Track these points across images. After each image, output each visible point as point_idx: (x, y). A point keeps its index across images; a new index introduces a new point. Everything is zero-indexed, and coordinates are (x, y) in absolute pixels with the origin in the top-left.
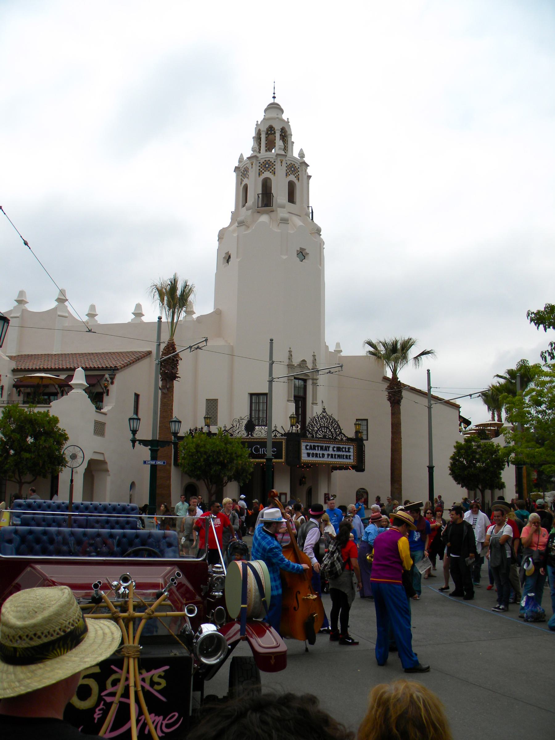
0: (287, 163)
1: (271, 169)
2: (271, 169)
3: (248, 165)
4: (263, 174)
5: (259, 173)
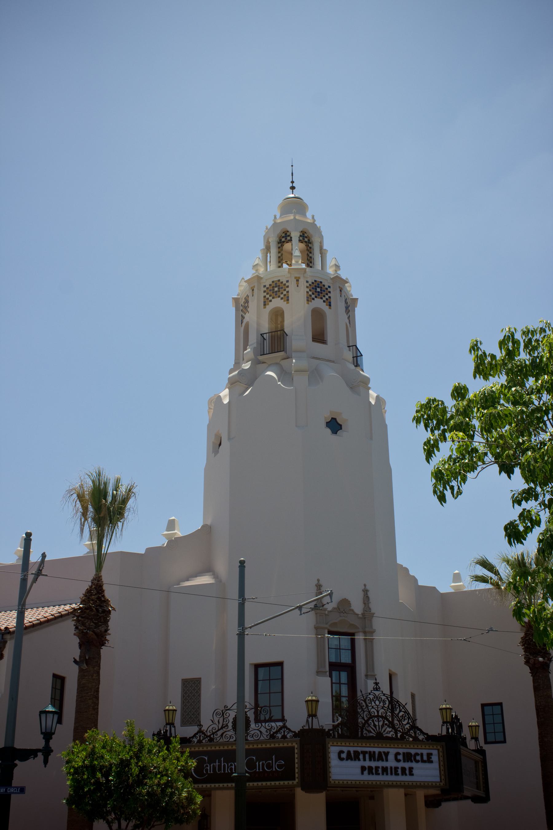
1: (282, 293)
2: (282, 293)
4: (270, 303)
5: (265, 302)
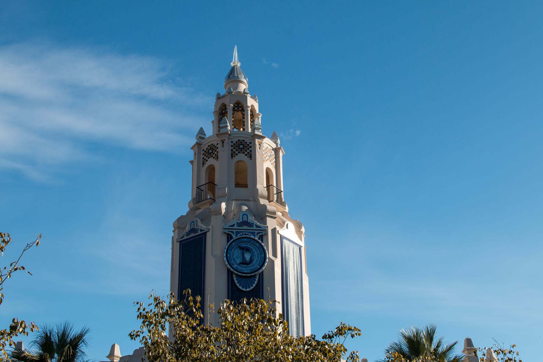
0: (217, 144)
1: (246, 151)
2: (246, 151)
3: (215, 143)
4: (236, 156)
5: (232, 154)
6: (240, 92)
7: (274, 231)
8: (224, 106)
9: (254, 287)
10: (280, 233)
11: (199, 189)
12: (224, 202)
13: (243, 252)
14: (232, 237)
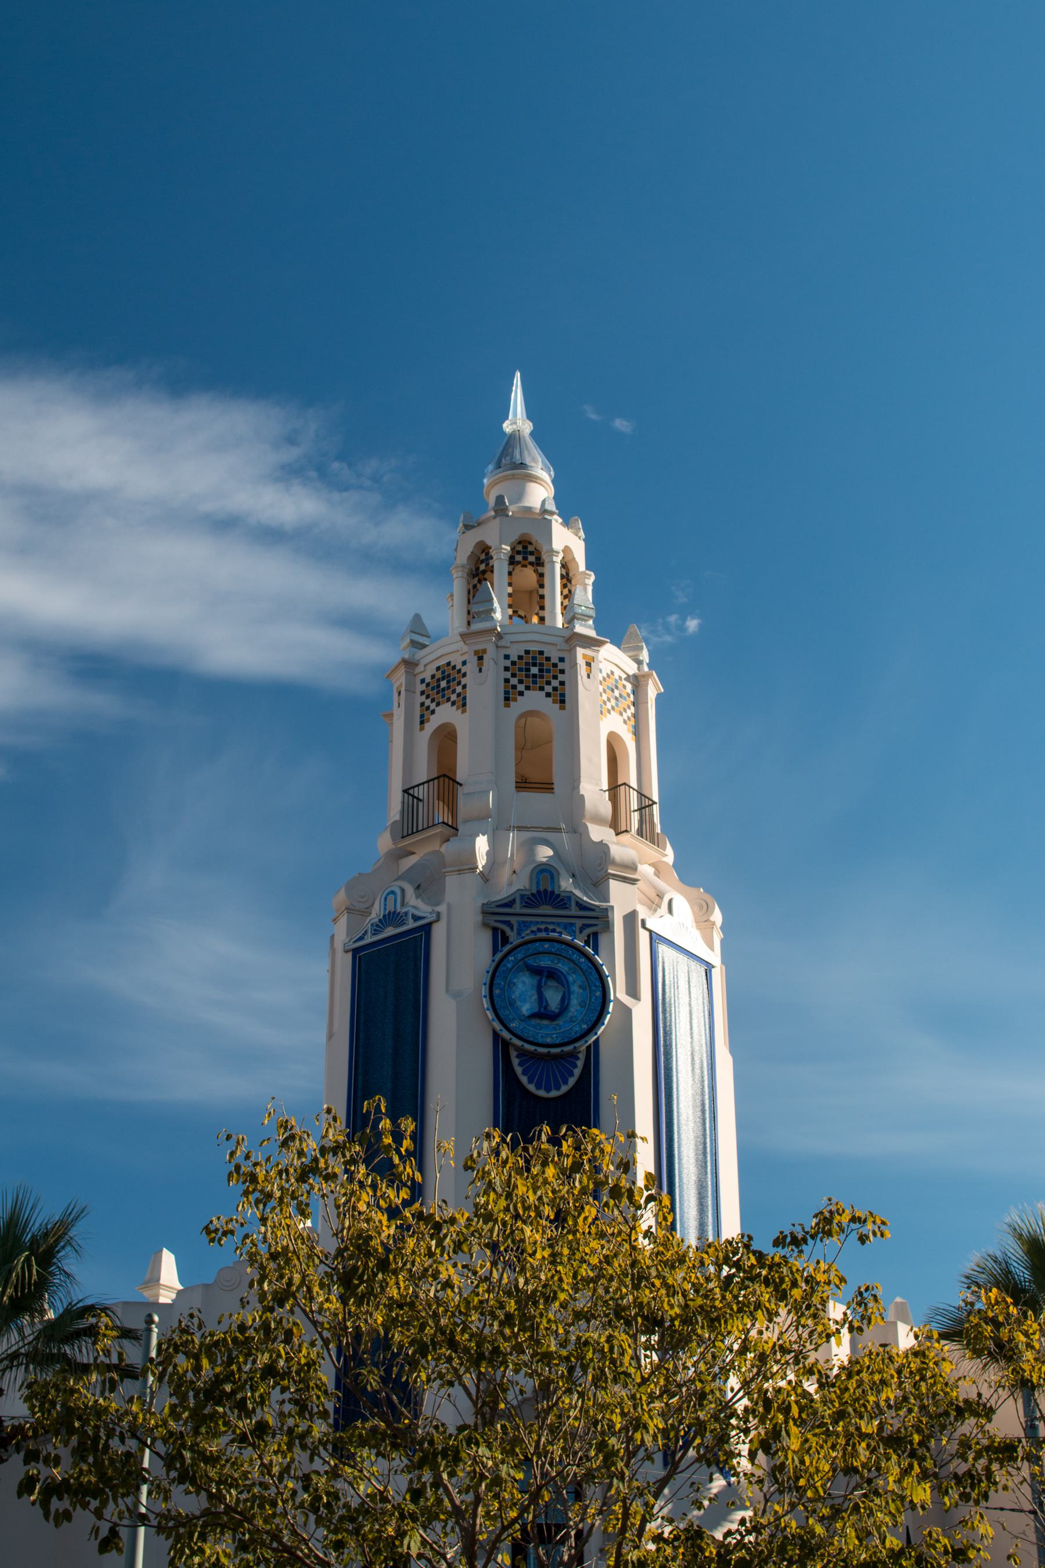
0: (464, 663)
1: (548, 683)
2: (548, 683)
3: (457, 660)
4: (519, 698)
5: (506, 692)
6: (529, 509)
7: (631, 919)
8: (483, 552)
9: (572, 1089)
10: (648, 926)
11: (409, 794)
12: (484, 835)
13: (540, 982)
14: (508, 937)
